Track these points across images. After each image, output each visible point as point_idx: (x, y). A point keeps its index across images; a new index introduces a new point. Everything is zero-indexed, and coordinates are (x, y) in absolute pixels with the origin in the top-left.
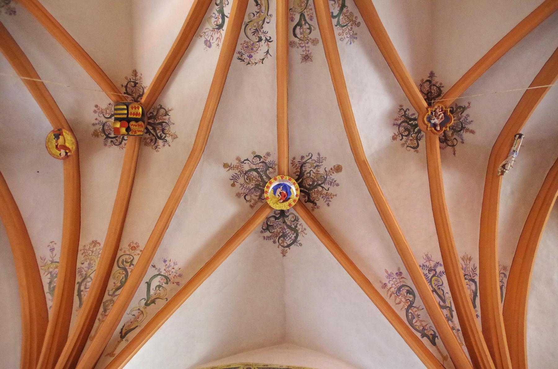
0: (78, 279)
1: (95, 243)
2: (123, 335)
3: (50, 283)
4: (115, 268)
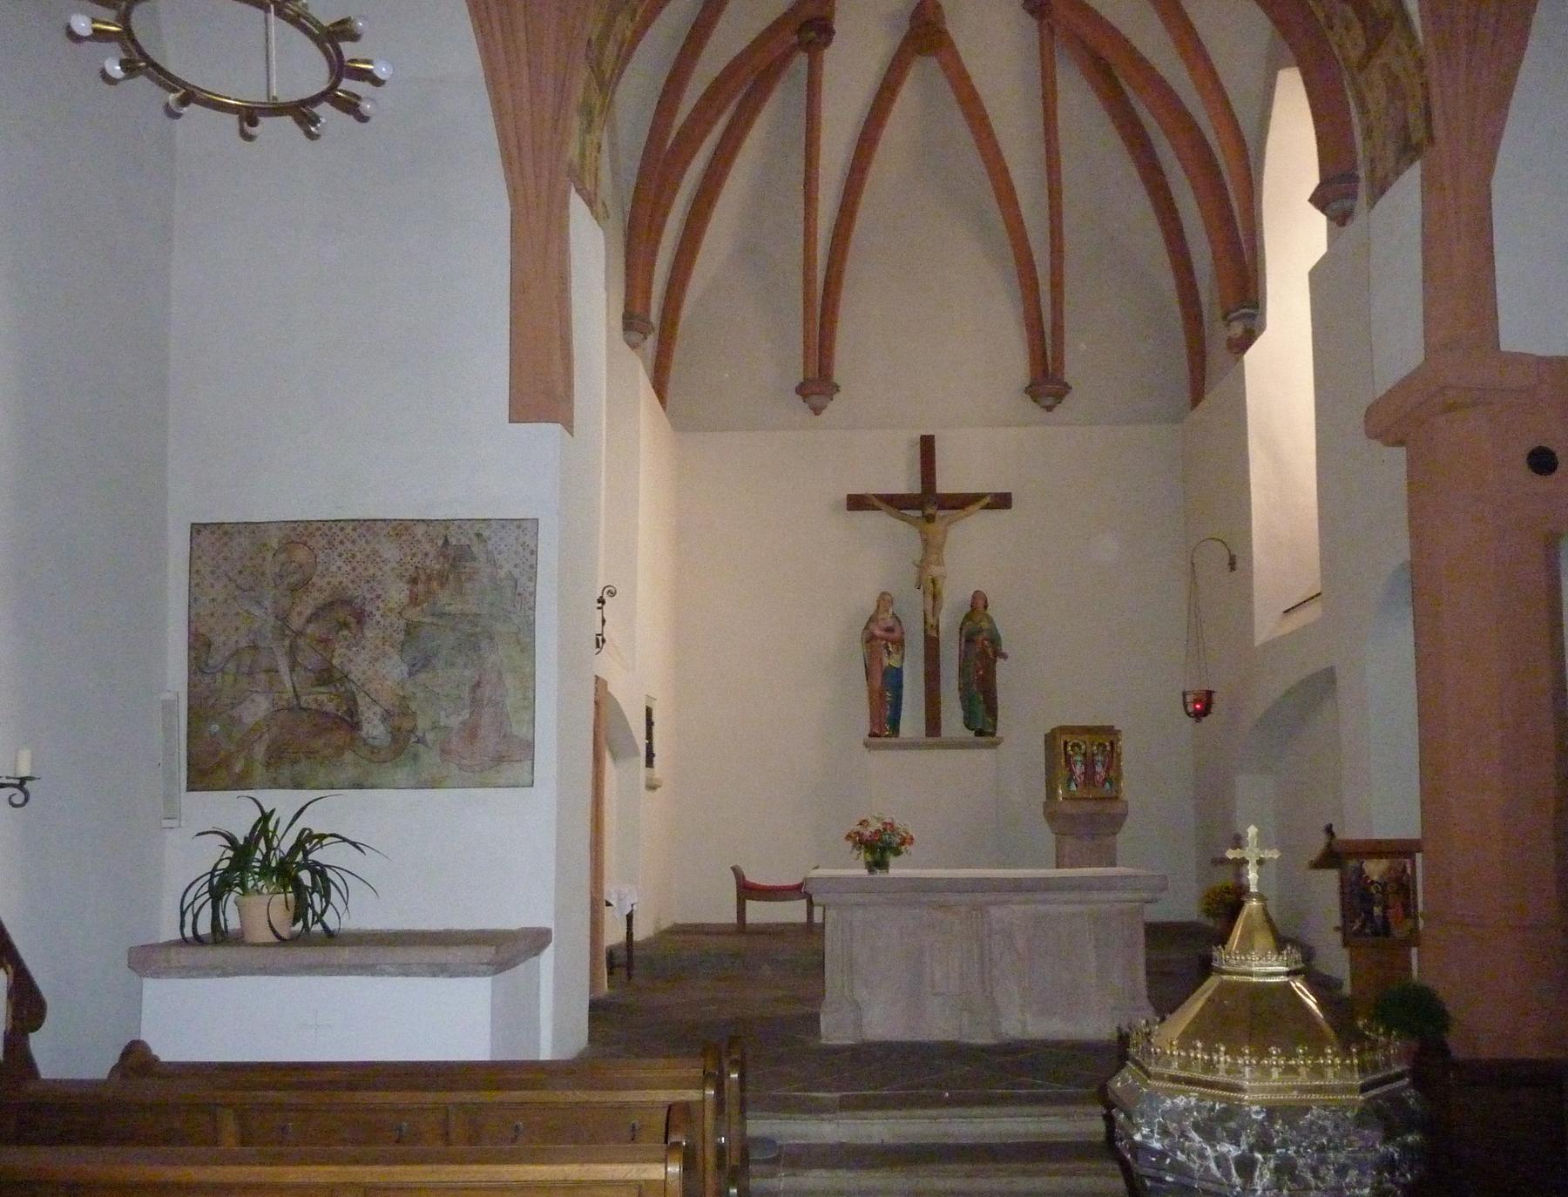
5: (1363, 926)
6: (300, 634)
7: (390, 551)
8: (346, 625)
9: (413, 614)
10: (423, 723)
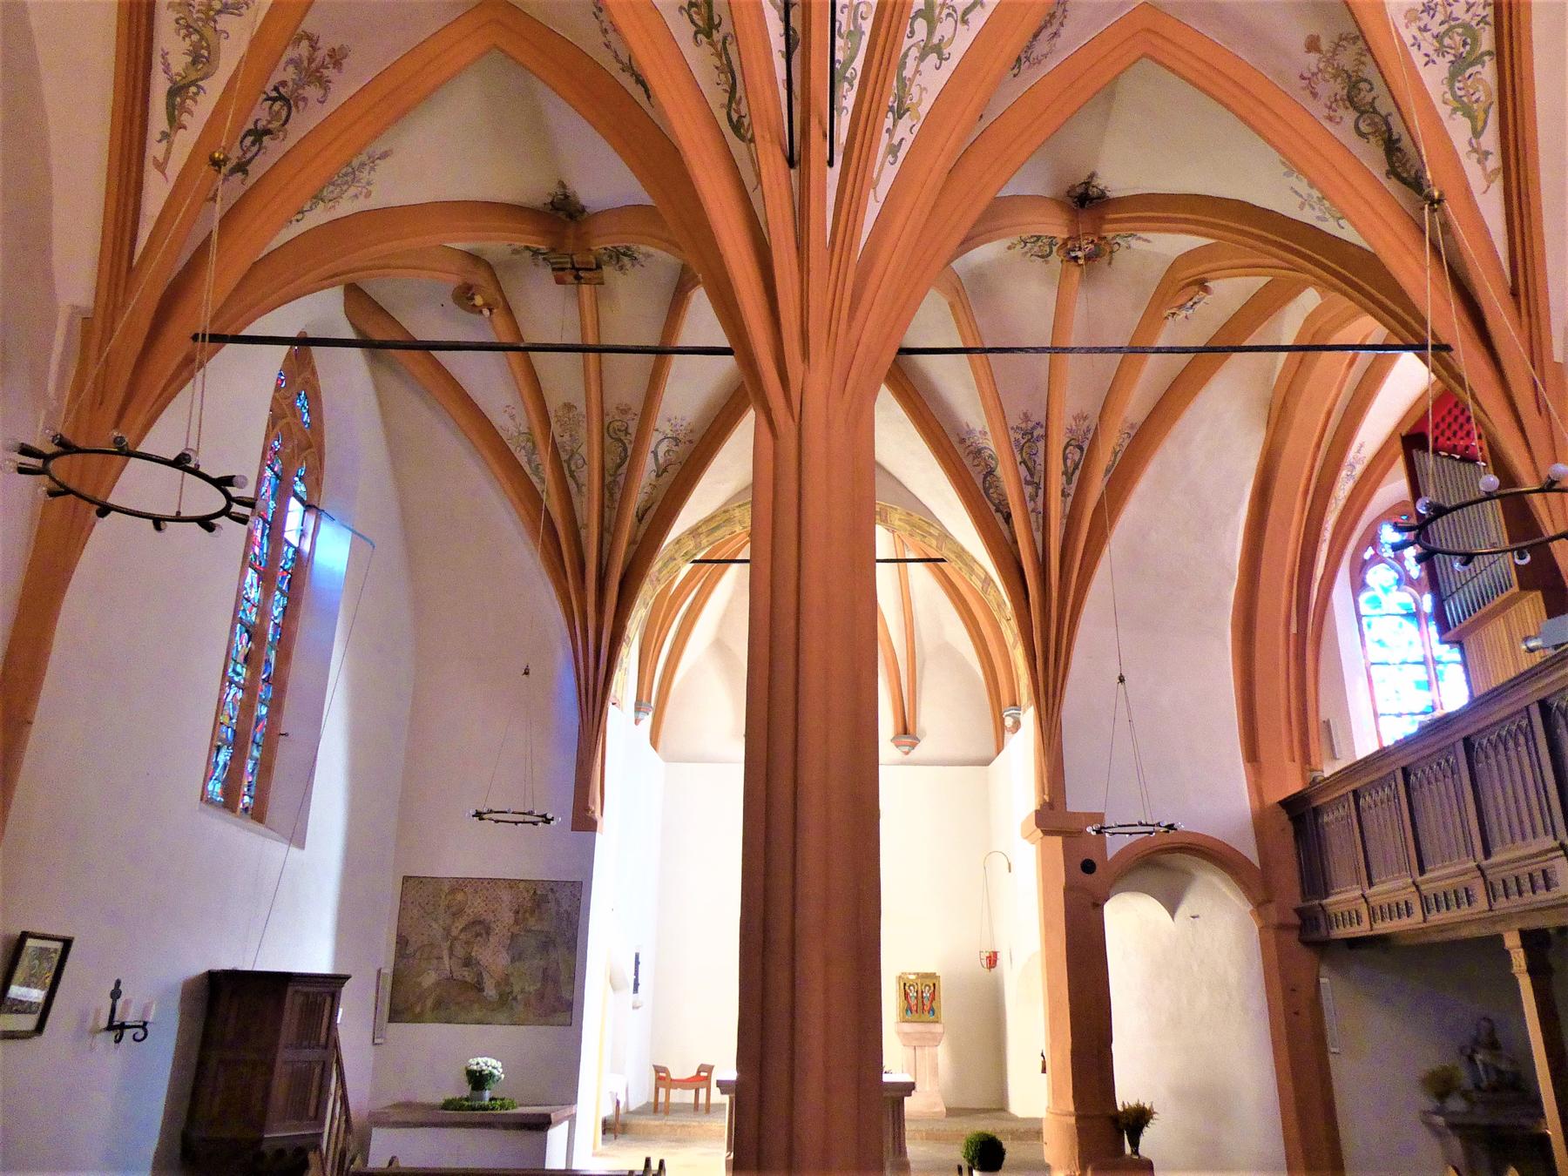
0: (564, 456)
1: (569, 407)
3: (529, 462)
4: (608, 441)
6: (456, 938)
7: (506, 896)
8: (477, 935)
9: (516, 930)
10: (516, 989)
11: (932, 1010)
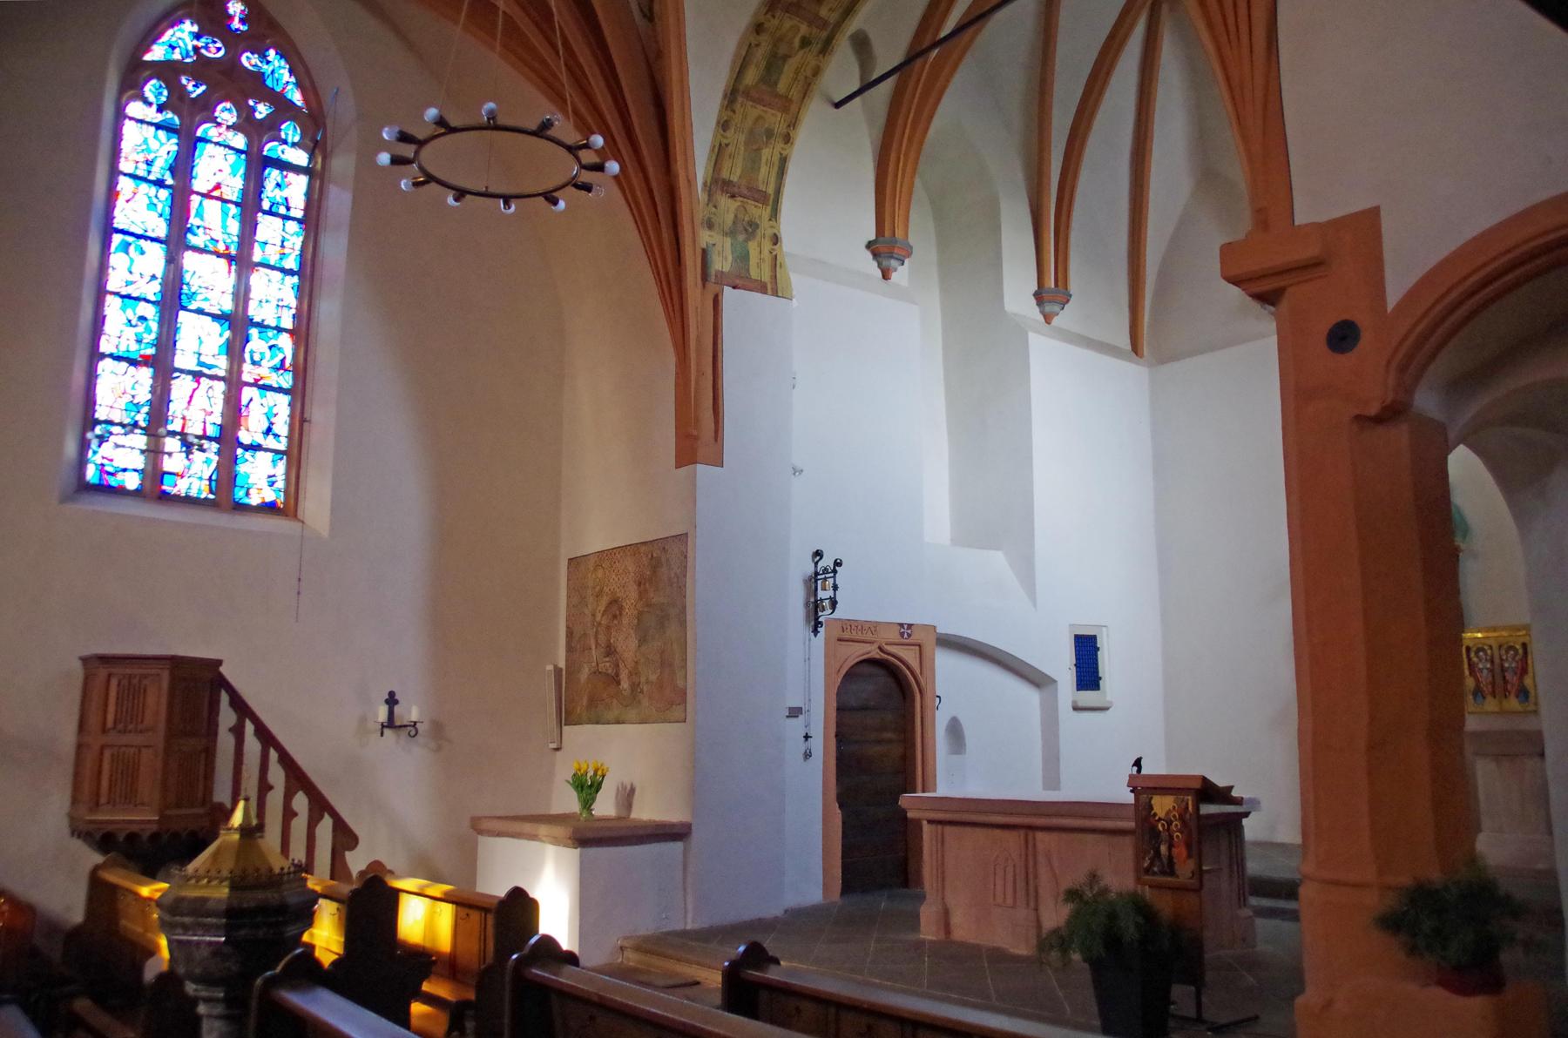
2: (649, 16)
5: (1152, 864)
8: (615, 617)
10: (643, 680)
11: (1523, 693)
